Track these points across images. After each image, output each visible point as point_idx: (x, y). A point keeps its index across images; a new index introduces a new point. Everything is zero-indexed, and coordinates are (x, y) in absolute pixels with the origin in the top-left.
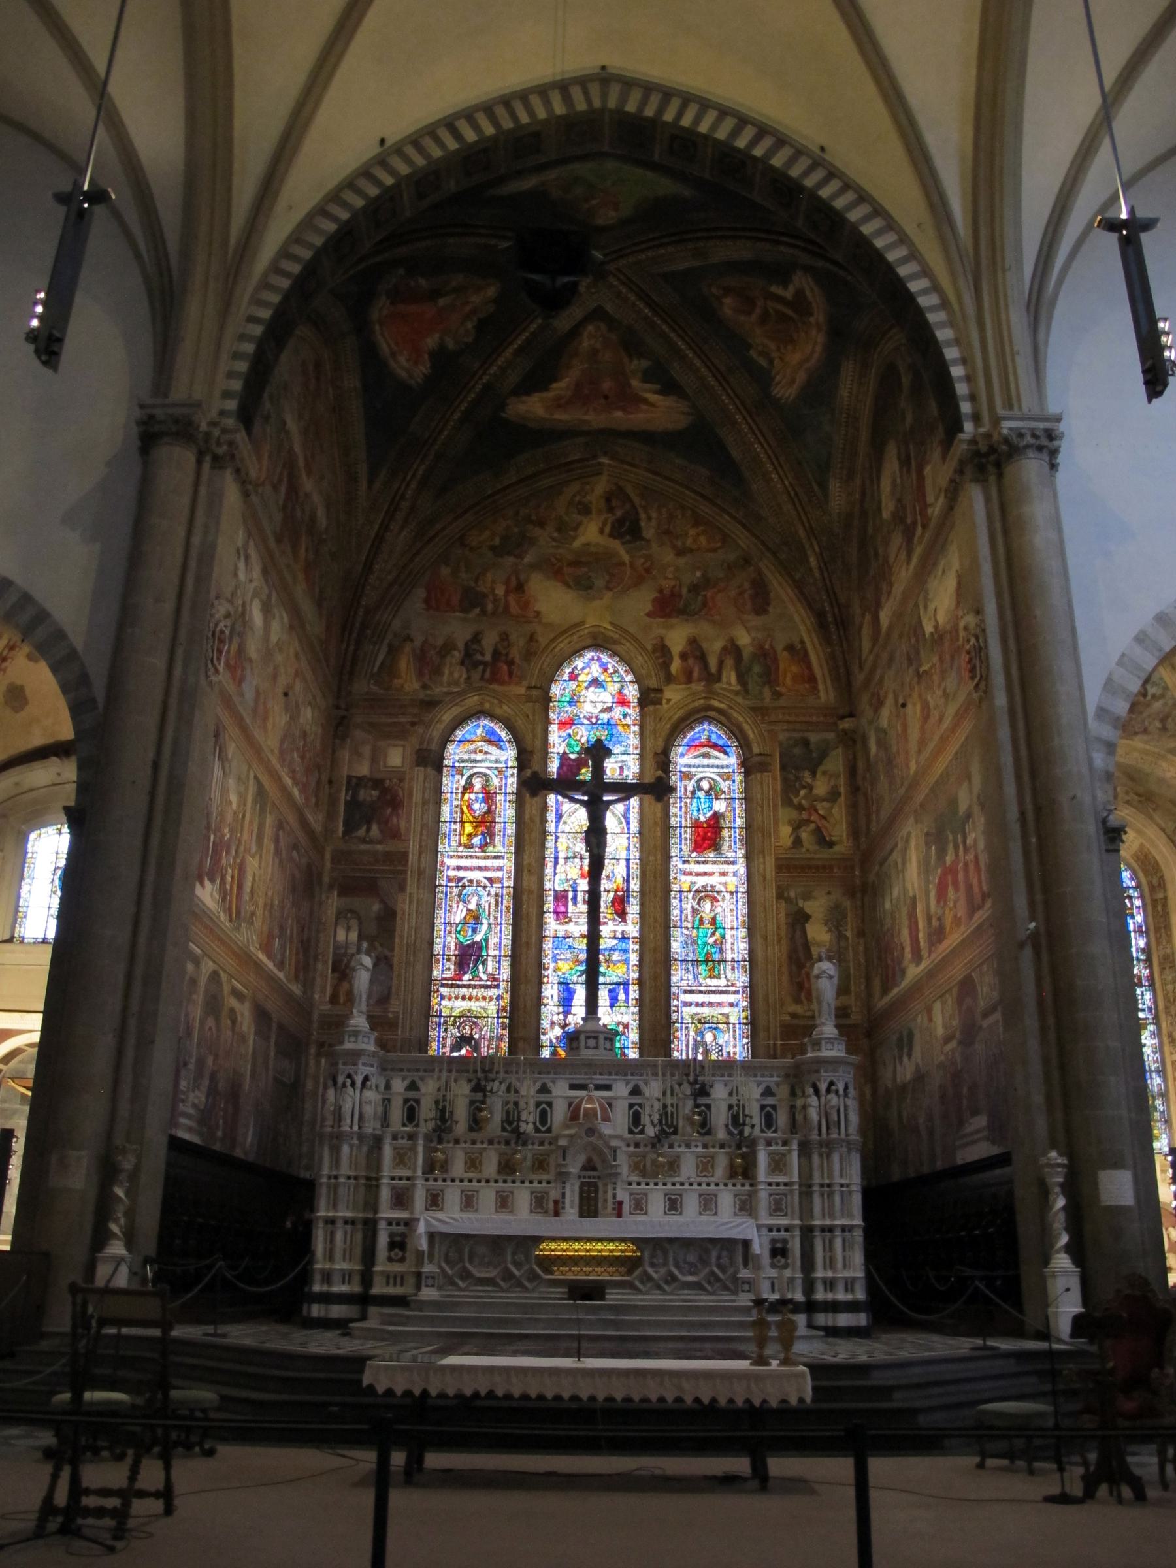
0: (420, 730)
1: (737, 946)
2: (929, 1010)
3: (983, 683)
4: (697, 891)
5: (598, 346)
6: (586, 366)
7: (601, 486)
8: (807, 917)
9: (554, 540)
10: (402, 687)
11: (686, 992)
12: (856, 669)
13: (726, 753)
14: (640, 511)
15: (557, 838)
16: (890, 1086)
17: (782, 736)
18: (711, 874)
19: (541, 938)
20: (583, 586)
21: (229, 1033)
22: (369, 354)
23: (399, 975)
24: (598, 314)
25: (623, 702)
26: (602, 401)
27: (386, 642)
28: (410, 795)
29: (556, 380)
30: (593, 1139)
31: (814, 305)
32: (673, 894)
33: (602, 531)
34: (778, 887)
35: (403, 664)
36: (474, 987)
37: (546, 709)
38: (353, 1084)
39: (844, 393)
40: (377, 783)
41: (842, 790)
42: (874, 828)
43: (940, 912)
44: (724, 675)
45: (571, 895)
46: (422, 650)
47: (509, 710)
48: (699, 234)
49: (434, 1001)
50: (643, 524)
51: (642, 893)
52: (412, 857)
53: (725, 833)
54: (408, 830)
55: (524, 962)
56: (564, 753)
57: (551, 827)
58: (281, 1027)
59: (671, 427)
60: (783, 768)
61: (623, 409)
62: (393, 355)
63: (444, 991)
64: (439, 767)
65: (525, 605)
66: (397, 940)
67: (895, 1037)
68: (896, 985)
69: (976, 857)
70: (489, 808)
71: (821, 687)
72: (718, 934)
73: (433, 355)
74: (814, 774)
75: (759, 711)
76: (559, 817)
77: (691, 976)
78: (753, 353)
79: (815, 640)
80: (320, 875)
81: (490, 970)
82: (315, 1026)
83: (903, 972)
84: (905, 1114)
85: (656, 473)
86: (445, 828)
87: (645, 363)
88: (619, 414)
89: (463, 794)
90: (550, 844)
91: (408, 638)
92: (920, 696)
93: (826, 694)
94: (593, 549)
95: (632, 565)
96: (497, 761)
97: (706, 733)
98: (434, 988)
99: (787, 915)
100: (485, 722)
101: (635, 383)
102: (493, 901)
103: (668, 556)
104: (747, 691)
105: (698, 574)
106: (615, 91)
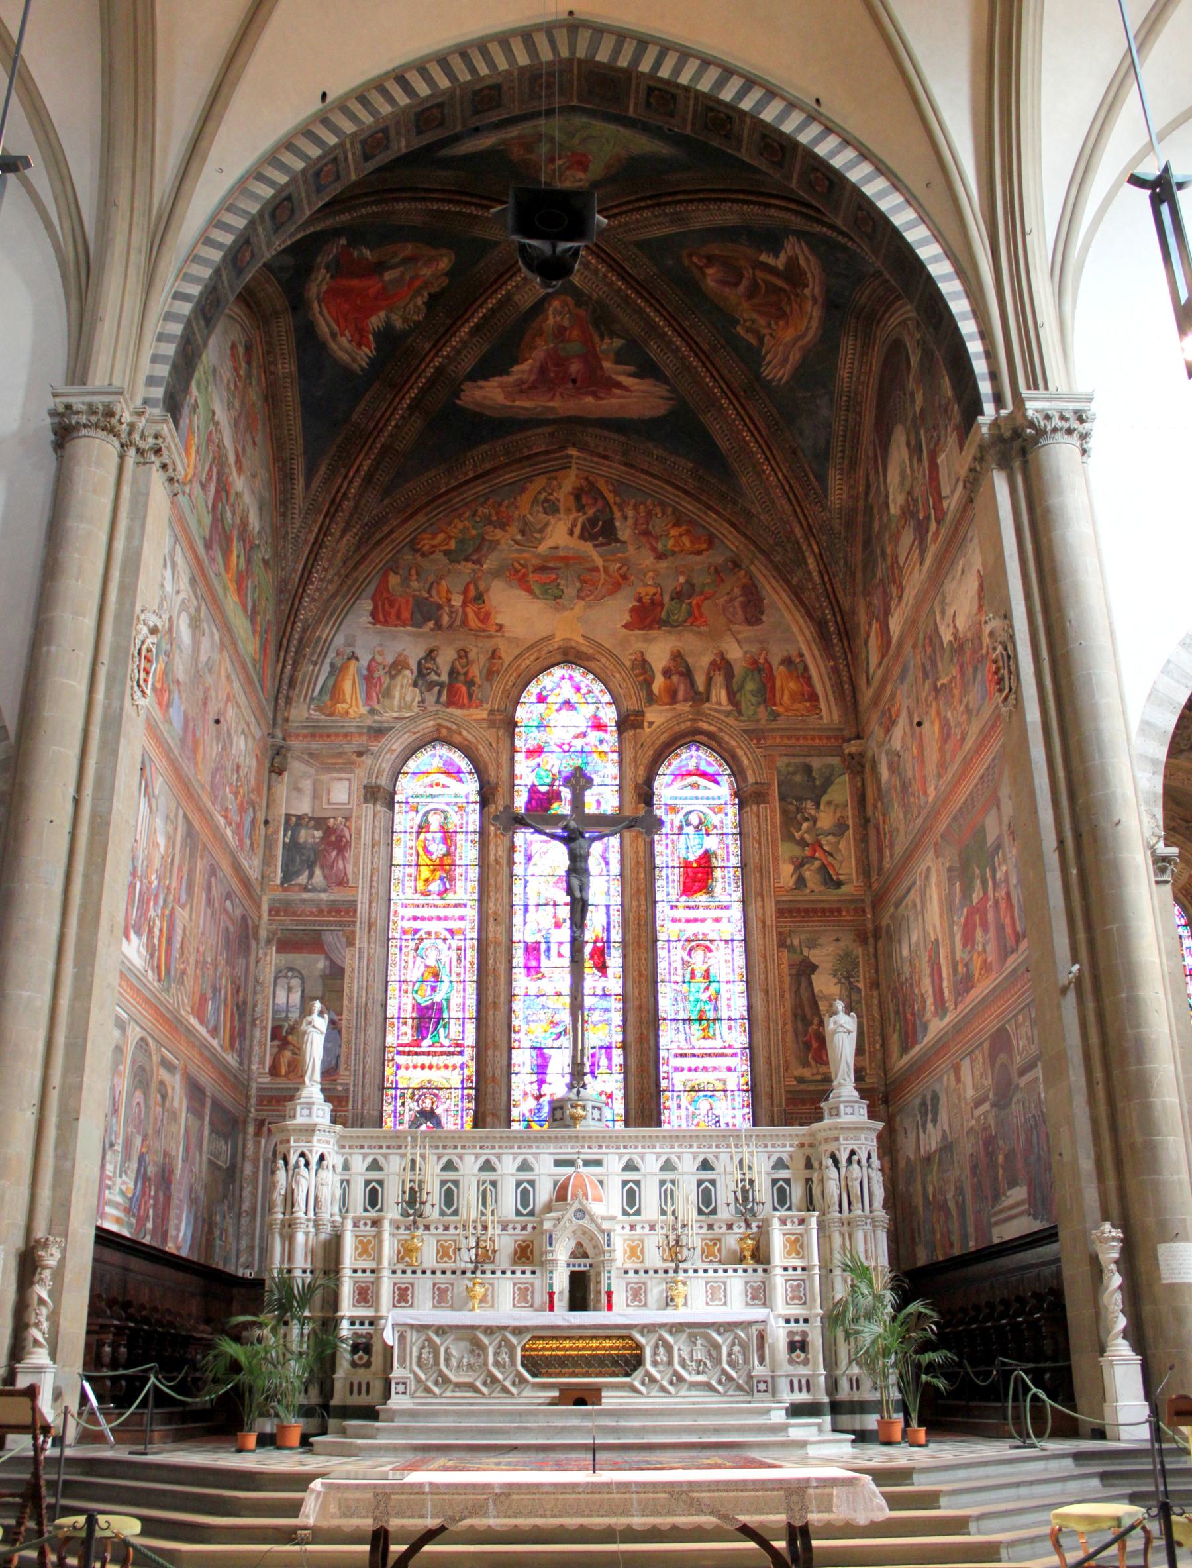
0: (367, 760)
1: (735, 1002)
2: (957, 1069)
3: (1012, 696)
4: (688, 940)
5: (566, 323)
7: (570, 481)
8: (813, 968)
9: (517, 543)
11: (676, 1055)
12: (863, 682)
13: (717, 783)
14: (615, 509)
15: (526, 882)
16: (912, 1157)
17: (781, 762)
18: (703, 920)
19: (510, 997)
20: (554, 595)
21: (159, 1109)
22: (307, 338)
23: (349, 1042)
25: (598, 726)
26: (570, 385)
27: (328, 661)
28: (358, 838)
29: (516, 361)
30: (585, 1222)
32: (659, 944)
33: (571, 533)
34: (780, 934)
35: (347, 686)
36: (435, 1054)
37: (512, 736)
38: (307, 1164)
39: (844, 373)
40: (320, 823)
41: (850, 822)
42: (887, 865)
43: (967, 958)
44: (713, 693)
45: (543, 947)
46: (369, 668)
47: (470, 737)
48: (681, 197)
49: (389, 1071)
50: (617, 524)
51: (624, 942)
52: (361, 908)
53: (718, 874)
54: (356, 874)
55: (491, 1023)
56: (534, 786)
57: (518, 870)
58: (216, 1104)
59: (648, 414)
60: (782, 798)
61: (594, 395)
62: (334, 335)
63: (401, 1060)
64: (391, 804)
65: (485, 618)
66: (346, 1002)
67: (917, 1102)
68: (914, 1043)
69: (1008, 894)
70: (449, 848)
71: (823, 705)
72: (711, 991)
73: (378, 335)
74: (817, 805)
75: (755, 735)
76: (529, 858)
77: (682, 1037)
79: (816, 653)
80: (256, 928)
81: (452, 1035)
82: (253, 1101)
83: (925, 1028)
84: (930, 1190)
85: (632, 466)
86: (397, 873)
87: (618, 343)
88: (590, 399)
89: (418, 833)
90: (518, 888)
91: (354, 657)
92: (938, 713)
93: (830, 713)
94: (561, 553)
95: (606, 569)
96: (456, 796)
97: (694, 760)
98: (388, 1056)
99: (791, 966)
100: (444, 751)
101: (606, 365)
102: (455, 958)
103: (647, 560)
104: (740, 713)
105: (682, 579)
106: (584, 36)
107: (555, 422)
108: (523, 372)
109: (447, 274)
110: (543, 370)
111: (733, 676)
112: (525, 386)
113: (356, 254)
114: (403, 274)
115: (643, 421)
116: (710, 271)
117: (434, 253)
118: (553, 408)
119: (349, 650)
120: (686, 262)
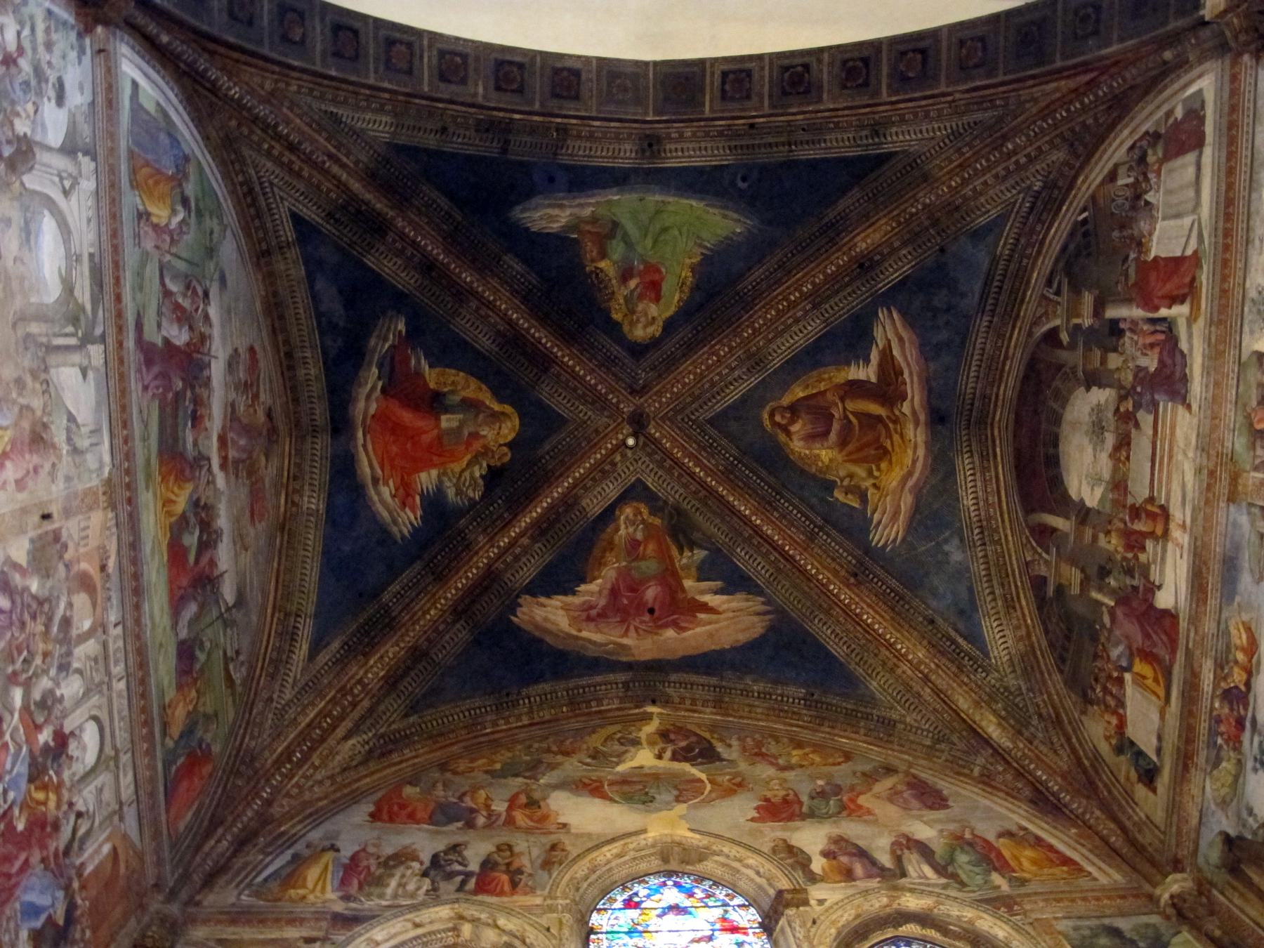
5: (639, 536)
6: (624, 564)
10: (304, 897)
24: (635, 492)
26: (647, 617)
27: (289, 853)
29: (583, 580)
31: (906, 375)
35: (313, 874)
39: (968, 502)
59: (743, 638)
61: (676, 625)
62: (375, 481)
78: (839, 495)
87: (700, 554)
88: (670, 633)
94: (646, 771)
101: (688, 583)
104: (963, 884)
107: (629, 666)
108: (592, 594)
109: (510, 445)
110: (614, 592)
111: (933, 852)
112: (594, 612)
113: (413, 362)
114: (462, 424)
115: (734, 649)
116: (795, 428)
117: (496, 407)
118: (623, 647)
119: (327, 843)
120: (767, 423)
